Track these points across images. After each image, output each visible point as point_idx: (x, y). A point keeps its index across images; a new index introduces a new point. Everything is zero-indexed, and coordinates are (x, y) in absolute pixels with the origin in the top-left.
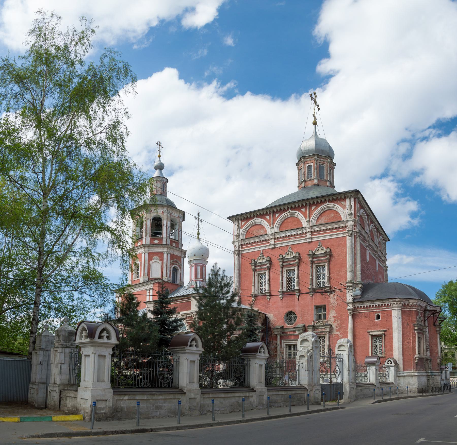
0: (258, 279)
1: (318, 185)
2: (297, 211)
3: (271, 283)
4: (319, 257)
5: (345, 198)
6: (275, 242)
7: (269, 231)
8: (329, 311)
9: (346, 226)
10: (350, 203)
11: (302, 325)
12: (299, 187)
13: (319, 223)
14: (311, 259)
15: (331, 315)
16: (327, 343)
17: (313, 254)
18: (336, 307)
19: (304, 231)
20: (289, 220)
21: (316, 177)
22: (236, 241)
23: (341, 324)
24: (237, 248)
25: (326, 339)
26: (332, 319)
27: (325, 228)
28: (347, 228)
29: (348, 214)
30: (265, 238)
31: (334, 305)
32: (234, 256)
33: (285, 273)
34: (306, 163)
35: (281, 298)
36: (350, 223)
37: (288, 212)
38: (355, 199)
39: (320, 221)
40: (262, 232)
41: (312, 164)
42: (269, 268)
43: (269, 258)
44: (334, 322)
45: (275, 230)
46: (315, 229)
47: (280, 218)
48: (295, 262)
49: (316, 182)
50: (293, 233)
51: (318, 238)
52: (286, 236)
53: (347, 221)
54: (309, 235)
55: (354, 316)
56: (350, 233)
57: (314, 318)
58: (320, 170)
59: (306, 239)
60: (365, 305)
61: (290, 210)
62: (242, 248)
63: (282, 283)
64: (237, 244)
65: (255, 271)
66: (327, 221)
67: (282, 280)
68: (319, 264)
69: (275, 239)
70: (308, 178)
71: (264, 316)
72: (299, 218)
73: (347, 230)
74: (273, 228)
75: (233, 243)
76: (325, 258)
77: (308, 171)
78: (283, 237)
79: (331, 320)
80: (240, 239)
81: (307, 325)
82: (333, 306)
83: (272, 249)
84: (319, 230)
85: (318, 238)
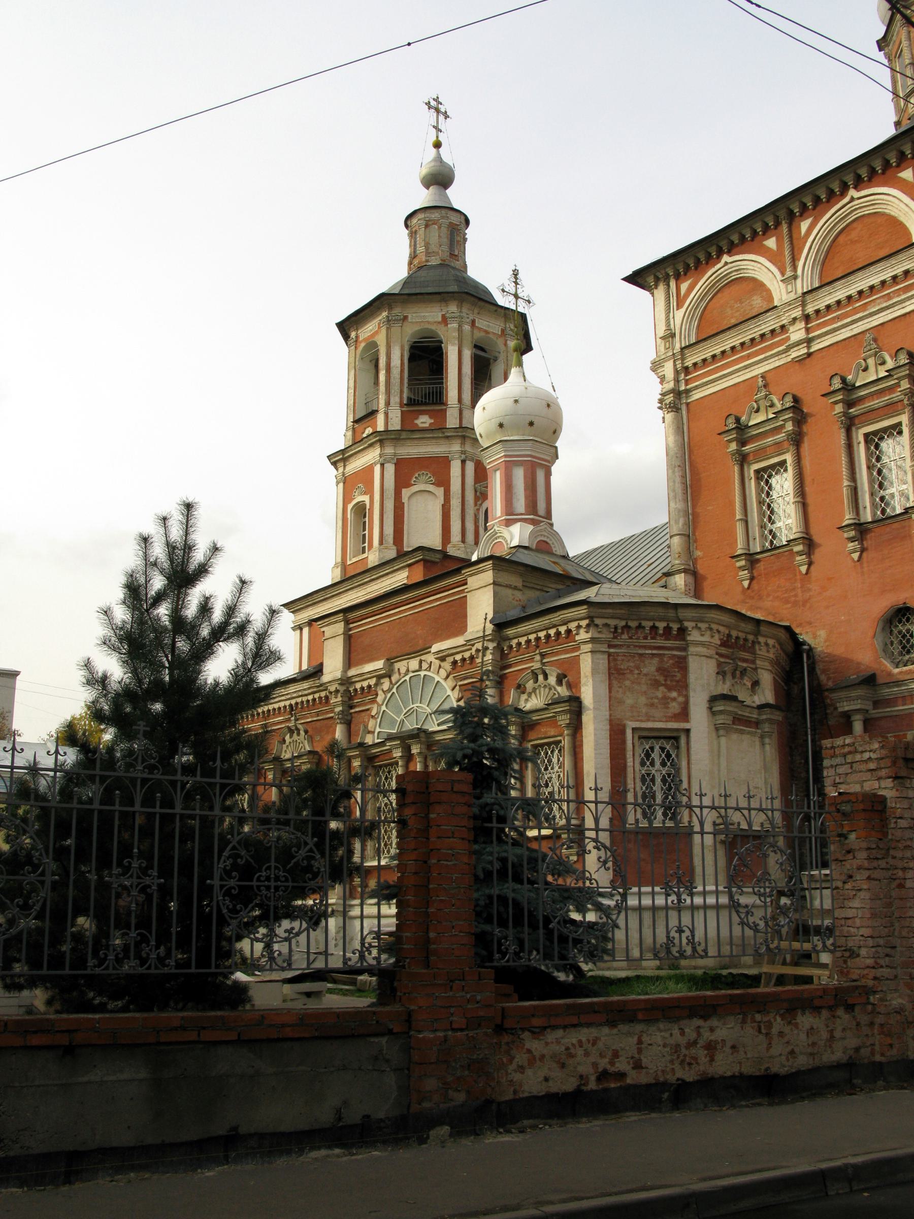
3: (810, 500)
6: (808, 330)
7: (780, 293)
20: (854, 235)
22: (665, 360)
24: (671, 385)
30: (769, 324)
33: (862, 447)
35: (856, 556)
40: (758, 303)
42: (797, 440)
45: (801, 286)
48: (896, 396)
50: (875, 280)
61: (852, 193)
62: (687, 384)
63: (855, 491)
64: (668, 369)
65: (743, 460)
69: (807, 318)
71: (783, 635)
72: (894, 212)
74: (795, 277)
75: (656, 366)
78: (838, 302)
80: (677, 347)
83: (800, 361)
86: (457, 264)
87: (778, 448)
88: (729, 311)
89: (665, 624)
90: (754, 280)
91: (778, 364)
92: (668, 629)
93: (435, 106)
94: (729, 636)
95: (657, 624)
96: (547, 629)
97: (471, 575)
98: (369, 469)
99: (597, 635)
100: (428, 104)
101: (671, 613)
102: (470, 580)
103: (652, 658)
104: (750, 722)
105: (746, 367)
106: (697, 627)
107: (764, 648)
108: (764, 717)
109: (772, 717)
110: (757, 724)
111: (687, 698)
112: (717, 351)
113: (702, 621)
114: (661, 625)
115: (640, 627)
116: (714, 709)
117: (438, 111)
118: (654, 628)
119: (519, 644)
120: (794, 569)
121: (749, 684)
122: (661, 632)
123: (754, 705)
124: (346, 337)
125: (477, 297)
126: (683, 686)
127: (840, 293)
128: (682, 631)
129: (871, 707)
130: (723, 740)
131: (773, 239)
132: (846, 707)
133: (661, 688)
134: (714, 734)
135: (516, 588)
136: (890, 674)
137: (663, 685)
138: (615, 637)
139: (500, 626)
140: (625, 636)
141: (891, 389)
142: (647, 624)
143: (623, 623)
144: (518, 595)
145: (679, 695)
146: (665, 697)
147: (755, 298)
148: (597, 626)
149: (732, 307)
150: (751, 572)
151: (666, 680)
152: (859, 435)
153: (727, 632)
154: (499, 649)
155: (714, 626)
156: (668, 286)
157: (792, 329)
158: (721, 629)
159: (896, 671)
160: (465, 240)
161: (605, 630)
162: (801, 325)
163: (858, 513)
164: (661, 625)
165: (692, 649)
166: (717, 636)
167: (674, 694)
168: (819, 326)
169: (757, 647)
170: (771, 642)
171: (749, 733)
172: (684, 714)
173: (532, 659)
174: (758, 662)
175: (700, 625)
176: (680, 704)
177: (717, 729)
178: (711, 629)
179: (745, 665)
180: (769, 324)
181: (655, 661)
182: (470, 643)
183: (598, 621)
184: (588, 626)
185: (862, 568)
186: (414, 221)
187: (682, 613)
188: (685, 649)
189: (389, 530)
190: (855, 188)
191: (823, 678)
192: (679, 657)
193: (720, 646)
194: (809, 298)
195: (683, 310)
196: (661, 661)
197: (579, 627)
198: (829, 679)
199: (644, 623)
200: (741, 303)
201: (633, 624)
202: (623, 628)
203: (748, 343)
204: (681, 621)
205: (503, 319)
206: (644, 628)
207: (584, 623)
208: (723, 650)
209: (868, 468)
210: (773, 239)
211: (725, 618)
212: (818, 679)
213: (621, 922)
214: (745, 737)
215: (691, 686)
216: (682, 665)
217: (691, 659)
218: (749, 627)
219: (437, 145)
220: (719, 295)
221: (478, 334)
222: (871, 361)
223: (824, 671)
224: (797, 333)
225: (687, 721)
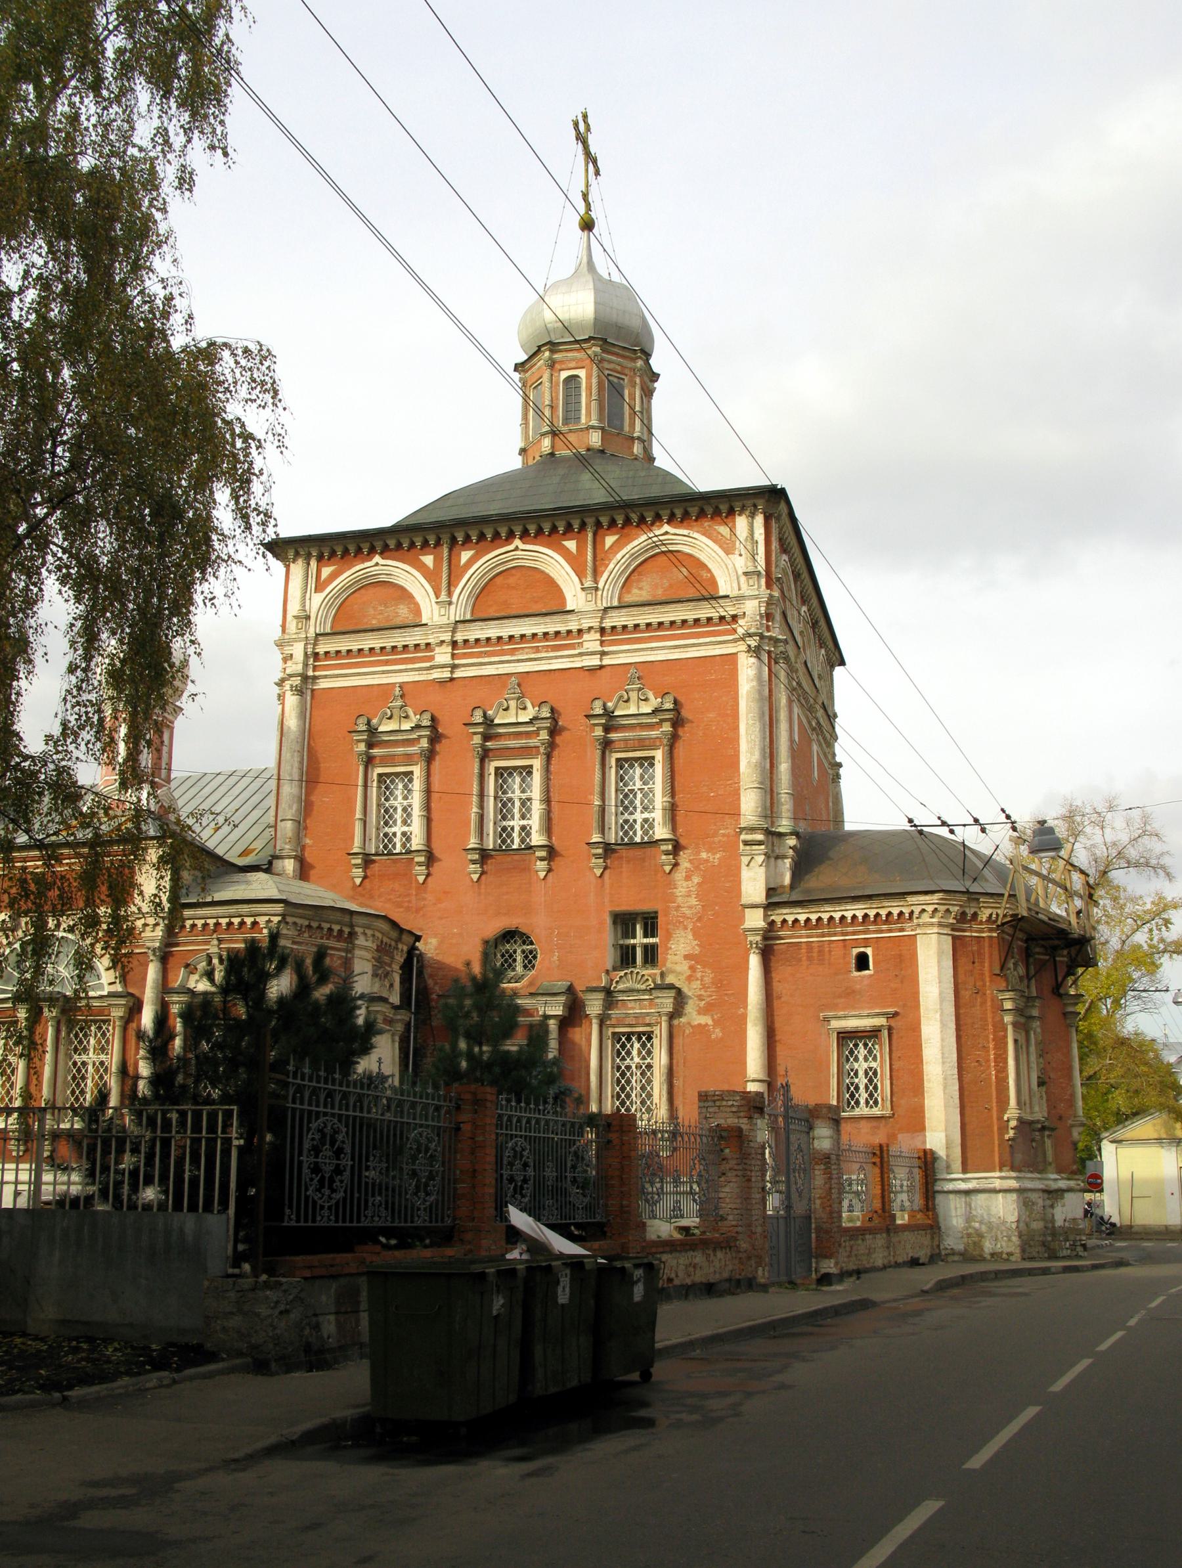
1: (602, 452)
2: (549, 546)
3: (435, 815)
4: (632, 727)
5: (731, 512)
6: (453, 656)
7: (430, 610)
8: (669, 936)
9: (735, 618)
10: (749, 528)
11: (562, 985)
12: (523, 451)
13: (628, 599)
14: (599, 732)
15: (679, 948)
16: (660, 1058)
17: (608, 714)
18: (700, 919)
19: (574, 627)
20: (512, 581)
21: (594, 423)
22: (295, 640)
23: (719, 984)
24: (299, 668)
25: (656, 1041)
26: (684, 967)
27: (654, 619)
28: (741, 622)
29: (746, 574)
30: (414, 637)
31: (688, 912)
32: (281, 697)
33: (492, 778)
34: (557, 366)
35: (475, 877)
36: (752, 608)
37: (511, 547)
38: (767, 520)
39: (635, 591)
40: (403, 613)
41: (582, 373)
42: (429, 757)
43: (427, 716)
44: (690, 979)
47: (478, 565)
48: (533, 742)
49: (595, 439)
50: (528, 631)
51: (624, 655)
52: (500, 638)
53: (740, 598)
54: (591, 642)
55: (767, 954)
56: (753, 643)
57: (609, 957)
58: (611, 394)
59: (581, 654)
60: (814, 917)
61: (517, 542)
62: (315, 668)
63: (481, 818)
64: (298, 650)
65: (369, 761)
66: (660, 594)
67: (481, 806)
68: (631, 755)
69: (454, 644)
70: (566, 421)
72: (553, 574)
73: (741, 631)
74: (450, 603)
76: (654, 733)
77: (567, 396)
79: (678, 968)
80: (311, 634)
81: (579, 987)
82: (684, 916)
83: (442, 683)
84: (630, 624)
85: (624, 655)
87: (408, 759)
90: (402, 589)
91: (417, 678)
92: (341, 932)
101: (347, 919)
105: (384, 672)
106: (365, 934)
112: (355, 647)
113: (368, 928)
114: (336, 928)
118: (330, 929)
120: (411, 877)
127: (492, 631)
128: (352, 935)
140: (306, 935)
141: (528, 734)
142: (326, 926)
143: (306, 923)
148: (287, 923)
149: (375, 609)
152: (492, 766)
156: (308, 564)
157: (438, 650)
163: (482, 839)
164: (336, 928)
165: (357, 952)
168: (465, 656)
173: (207, 942)
180: (414, 637)
183: (289, 919)
190: (521, 538)
191: (430, 982)
194: (460, 626)
198: (436, 983)
201: (315, 924)
203: (389, 649)
217: (356, 961)
220: (363, 591)
222: (513, 704)
223: (431, 976)
224: (443, 656)
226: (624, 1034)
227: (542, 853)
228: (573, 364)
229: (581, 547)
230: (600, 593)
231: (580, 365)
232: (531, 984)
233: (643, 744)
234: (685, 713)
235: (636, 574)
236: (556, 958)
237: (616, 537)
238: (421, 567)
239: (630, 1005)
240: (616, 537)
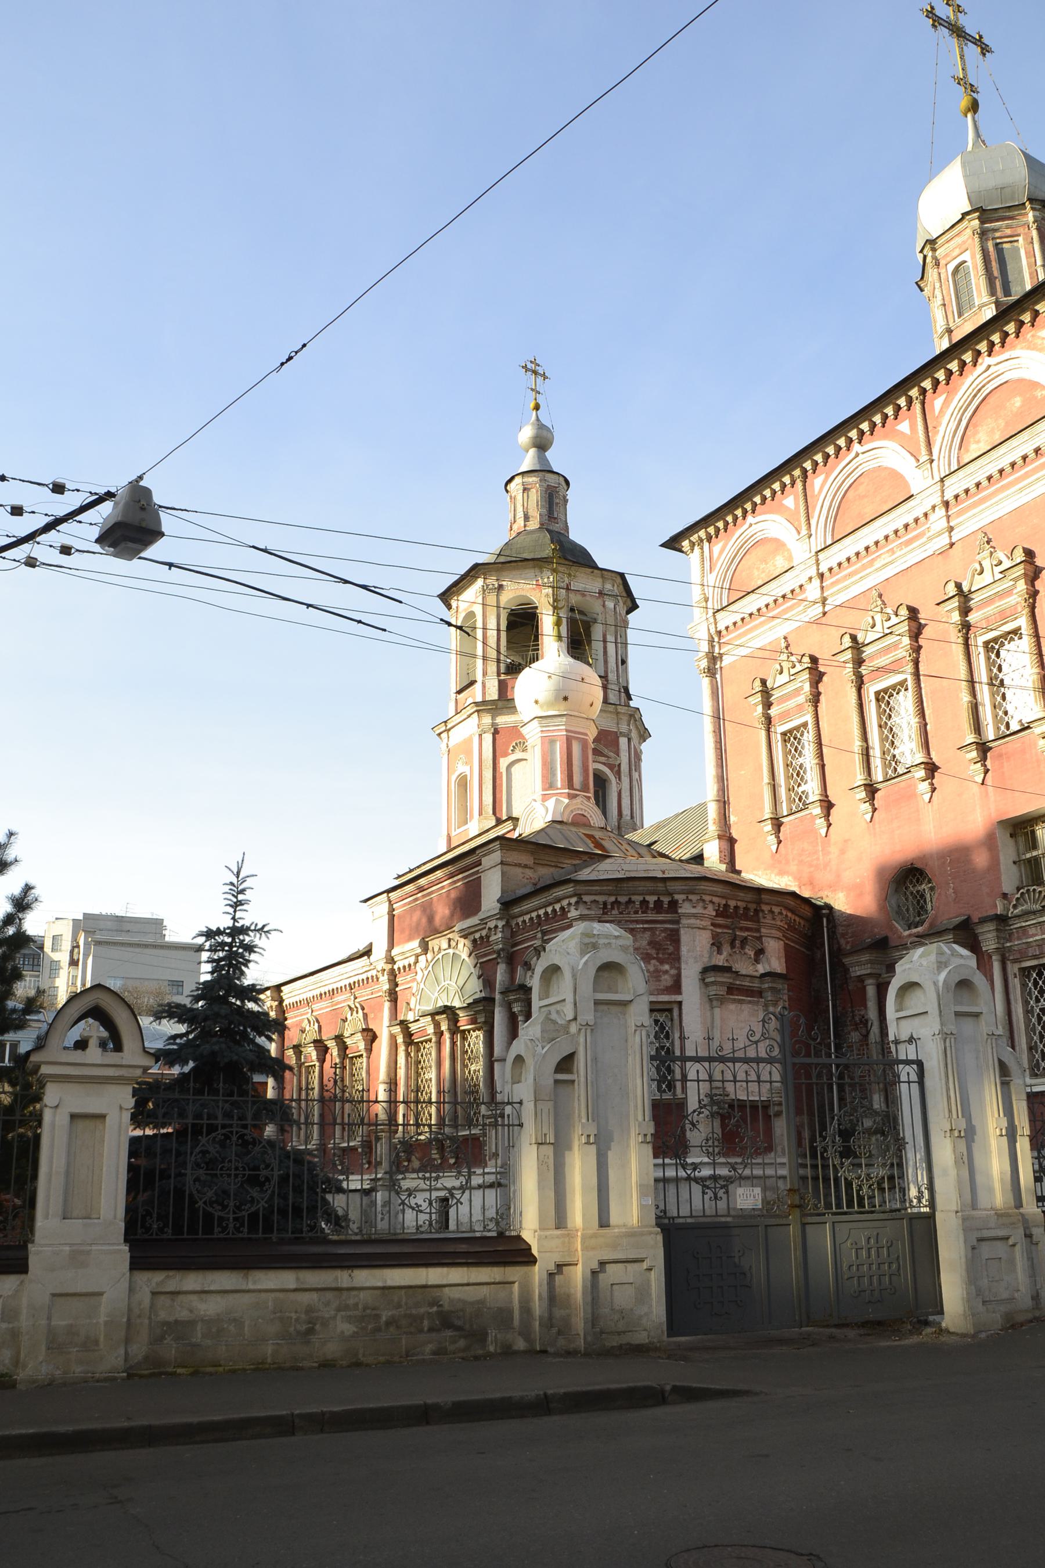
0: (786, 753)
2: (885, 437)
4: (989, 601)
19: (919, 513)
20: (862, 489)
35: (868, 817)
37: (852, 454)
46: (955, 486)
51: (971, 522)
59: (930, 539)
67: (865, 737)
85: (971, 522)
86: (556, 527)
88: (756, 573)
89: (655, 898)
90: (776, 540)
92: (658, 904)
93: (533, 370)
94: (726, 906)
95: (648, 898)
96: (545, 906)
97: (485, 855)
98: (468, 741)
99: (586, 912)
100: (525, 367)
101: (660, 886)
102: (484, 860)
103: (643, 932)
104: (752, 991)
107: (769, 916)
108: (766, 986)
109: (774, 985)
110: (760, 993)
111: (679, 969)
114: (652, 899)
115: (630, 901)
116: (707, 980)
117: (535, 372)
118: (644, 902)
119: (524, 921)
120: (814, 831)
121: (752, 954)
122: (652, 906)
123: (757, 974)
124: (449, 607)
125: (575, 558)
126: (675, 959)
128: (674, 905)
129: (884, 971)
130: (717, 1011)
131: (791, 498)
132: (857, 971)
133: (653, 962)
134: (707, 1006)
135: (526, 866)
136: (900, 937)
137: (654, 958)
138: (604, 913)
139: (507, 904)
142: (637, 899)
143: (612, 899)
144: (529, 873)
145: (671, 968)
146: (657, 971)
147: (777, 558)
148: (585, 902)
149: (758, 569)
150: (778, 837)
151: (657, 954)
153: (724, 902)
154: (508, 924)
155: (707, 898)
158: (716, 900)
159: (907, 933)
160: (566, 501)
161: (593, 906)
162: (816, 582)
163: (869, 774)
164: (652, 899)
165: (684, 921)
166: (710, 907)
167: (667, 967)
169: (761, 914)
170: (776, 910)
171: (750, 1002)
172: (676, 987)
173: (534, 938)
174: (763, 930)
175: (691, 897)
176: (672, 976)
177: (711, 1000)
178: (704, 901)
179: (745, 934)
181: (647, 935)
182: (484, 921)
183: (586, 898)
184: (577, 903)
185: (874, 829)
186: (512, 486)
187: (672, 886)
188: (678, 922)
189: (488, 799)
191: (842, 942)
192: (672, 930)
193: (716, 916)
194: (821, 556)
195: (714, 573)
196: (653, 934)
197: (569, 904)
198: (848, 942)
199: (634, 898)
200: (766, 564)
201: (623, 899)
202: (613, 904)
204: (671, 894)
205: (600, 580)
206: (634, 902)
207: (573, 900)
208: (720, 921)
209: (880, 726)
210: (791, 498)
211: (718, 889)
212: (838, 943)
213: (465, 1198)
214: (744, 1006)
215: (683, 959)
216: (674, 937)
217: (682, 932)
218: (749, 896)
219: (537, 407)
220: (747, 556)
221: (574, 599)
223: (843, 935)
225: (680, 993)
226: (1033, 968)
227: (921, 773)
228: (957, 251)
229: (913, 427)
230: (935, 464)
231: (964, 247)
232: (931, 925)
233: (1004, 616)
234: (1039, 562)
235: (970, 428)
236: (951, 891)
237: (944, 396)
238: (781, 510)
239: (1032, 931)
240: (944, 396)
